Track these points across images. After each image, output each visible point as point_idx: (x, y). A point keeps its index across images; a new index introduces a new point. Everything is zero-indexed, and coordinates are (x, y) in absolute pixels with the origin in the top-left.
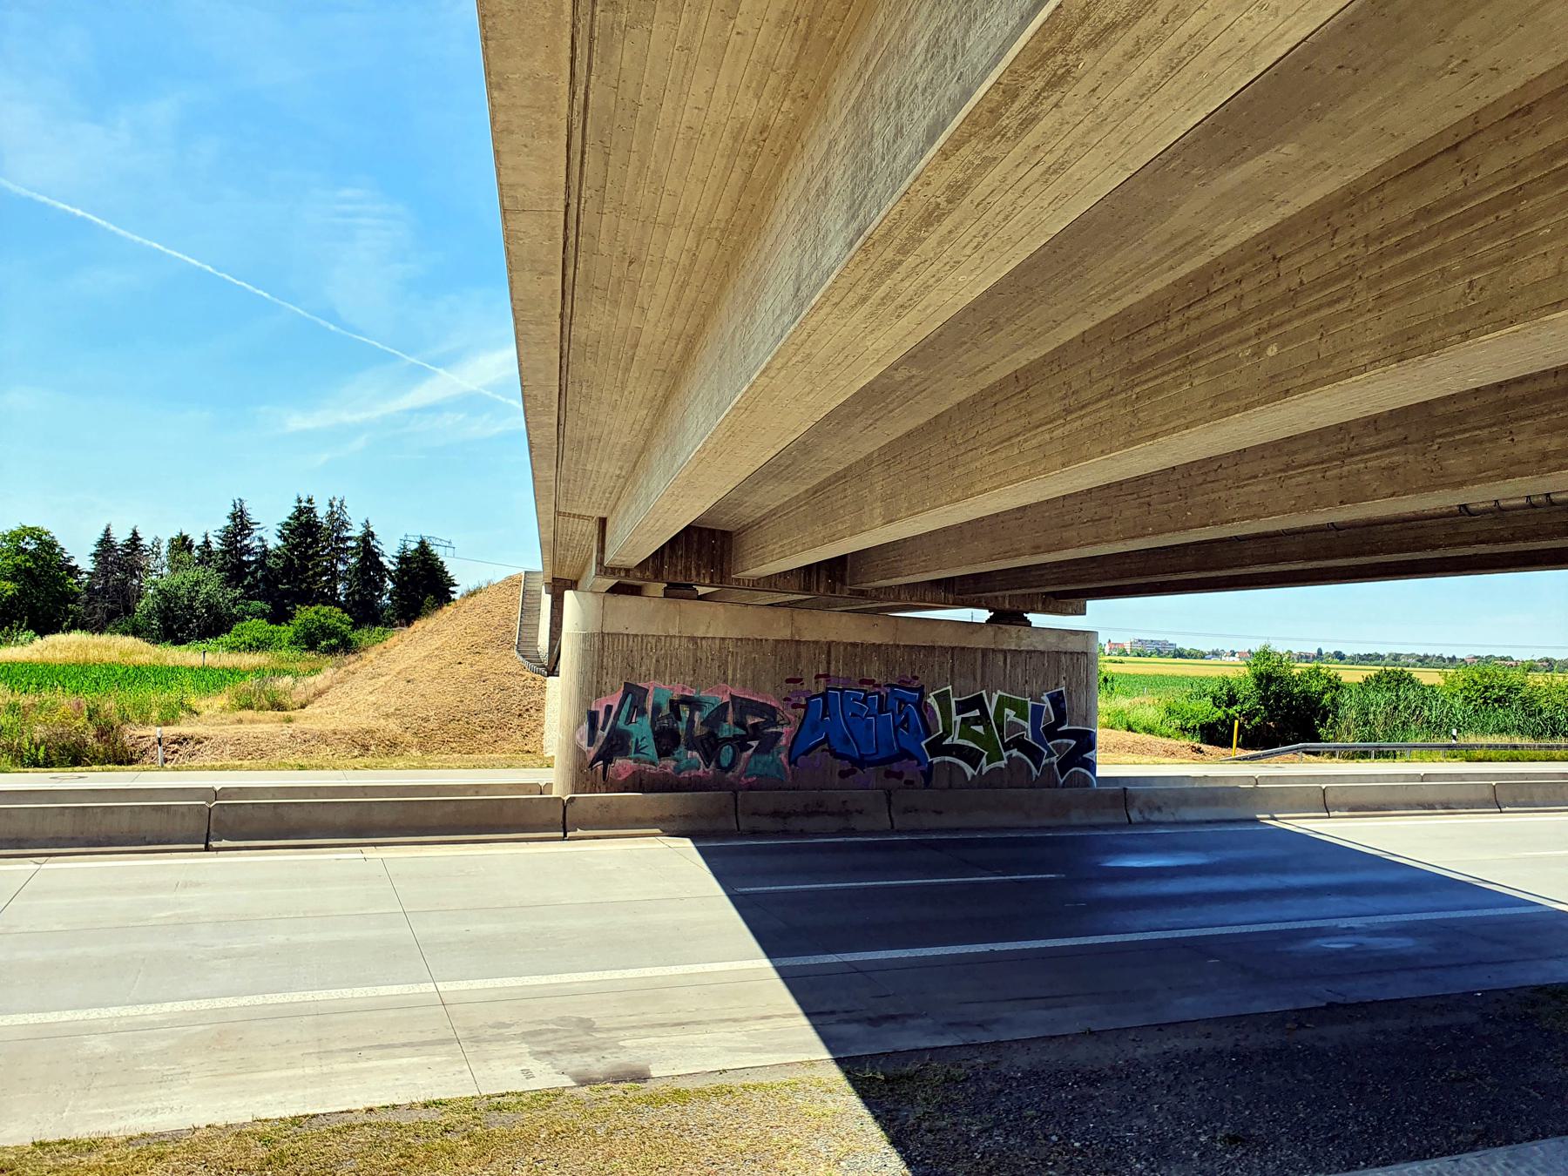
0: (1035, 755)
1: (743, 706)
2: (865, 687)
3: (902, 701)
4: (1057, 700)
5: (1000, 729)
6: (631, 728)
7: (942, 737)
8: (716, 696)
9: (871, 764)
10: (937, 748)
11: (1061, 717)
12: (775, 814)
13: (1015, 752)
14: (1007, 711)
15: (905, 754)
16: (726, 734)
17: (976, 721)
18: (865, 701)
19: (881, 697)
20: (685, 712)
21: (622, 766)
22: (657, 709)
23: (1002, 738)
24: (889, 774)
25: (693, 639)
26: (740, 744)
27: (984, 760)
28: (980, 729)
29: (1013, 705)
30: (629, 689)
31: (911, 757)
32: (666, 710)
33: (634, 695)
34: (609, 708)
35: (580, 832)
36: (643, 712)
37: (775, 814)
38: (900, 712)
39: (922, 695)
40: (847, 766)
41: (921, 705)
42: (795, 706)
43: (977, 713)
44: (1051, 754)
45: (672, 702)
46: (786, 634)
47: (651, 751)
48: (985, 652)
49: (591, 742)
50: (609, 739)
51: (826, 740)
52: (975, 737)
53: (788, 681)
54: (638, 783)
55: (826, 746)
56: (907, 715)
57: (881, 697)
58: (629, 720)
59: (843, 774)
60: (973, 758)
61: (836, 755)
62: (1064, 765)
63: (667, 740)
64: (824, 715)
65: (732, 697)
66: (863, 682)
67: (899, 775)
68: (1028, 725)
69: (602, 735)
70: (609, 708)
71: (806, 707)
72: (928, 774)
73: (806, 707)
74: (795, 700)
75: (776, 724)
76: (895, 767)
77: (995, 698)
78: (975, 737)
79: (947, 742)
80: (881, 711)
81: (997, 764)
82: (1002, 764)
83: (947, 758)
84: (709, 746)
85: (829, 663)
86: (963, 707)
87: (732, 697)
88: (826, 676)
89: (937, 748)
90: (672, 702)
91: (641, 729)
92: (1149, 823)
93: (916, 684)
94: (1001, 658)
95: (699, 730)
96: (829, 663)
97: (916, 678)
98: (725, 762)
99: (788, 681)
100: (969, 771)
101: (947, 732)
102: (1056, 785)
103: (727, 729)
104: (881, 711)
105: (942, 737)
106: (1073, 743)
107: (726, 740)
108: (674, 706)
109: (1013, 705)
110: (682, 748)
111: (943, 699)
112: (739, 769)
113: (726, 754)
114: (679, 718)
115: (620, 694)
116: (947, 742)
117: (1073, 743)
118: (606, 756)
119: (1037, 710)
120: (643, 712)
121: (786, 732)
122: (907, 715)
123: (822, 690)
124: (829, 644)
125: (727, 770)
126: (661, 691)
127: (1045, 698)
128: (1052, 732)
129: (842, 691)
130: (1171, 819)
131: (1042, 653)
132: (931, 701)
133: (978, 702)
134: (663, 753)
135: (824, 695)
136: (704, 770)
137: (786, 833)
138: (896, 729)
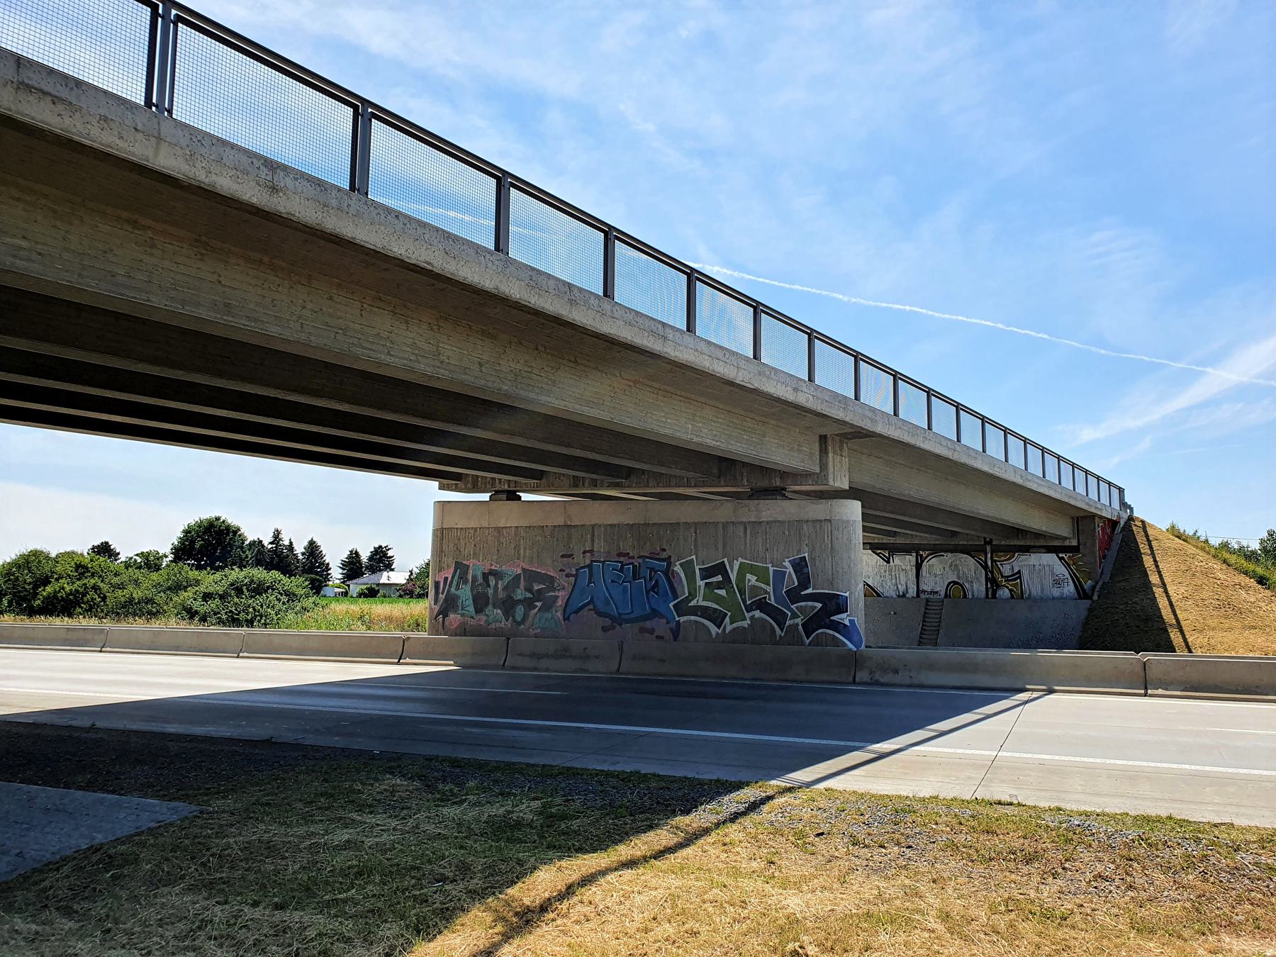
0: (779, 617)
1: (531, 576)
2: (622, 559)
3: (652, 569)
4: (799, 566)
5: (742, 592)
6: (458, 593)
7: (688, 600)
8: (513, 570)
9: (627, 621)
10: (682, 609)
11: (805, 581)
12: (534, 655)
13: (757, 614)
14: (748, 576)
15: (655, 614)
16: (519, 597)
17: (719, 586)
18: (621, 570)
19: (634, 567)
20: (492, 581)
21: (454, 618)
22: (475, 579)
23: (744, 602)
24: (642, 630)
25: (498, 529)
26: (529, 603)
27: (727, 619)
28: (723, 592)
29: (752, 569)
30: (458, 565)
31: (662, 616)
32: (480, 580)
33: (461, 568)
34: (446, 579)
35: (408, 660)
36: (466, 582)
37: (534, 655)
38: (651, 579)
39: (669, 565)
40: (608, 622)
41: (668, 573)
42: (567, 576)
43: (720, 578)
44: (794, 616)
45: (484, 574)
46: (561, 521)
47: (472, 609)
48: (725, 525)
49: (436, 603)
50: (446, 600)
51: (591, 601)
52: (718, 600)
53: (562, 556)
54: (463, 631)
55: (591, 607)
56: (657, 581)
57: (634, 567)
58: (457, 588)
59: (605, 629)
60: (717, 619)
61: (600, 614)
62: (809, 627)
63: (480, 603)
64: (590, 582)
65: (523, 569)
66: (620, 555)
67: (652, 631)
68: (770, 589)
69: (442, 597)
70: (446, 579)
71: (576, 576)
72: (676, 631)
73: (576, 576)
74: (568, 571)
75: (554, 590)
76: (648, 624)
77: (736, 567)
78: (718, 600)
79: (692, 604)
80: (635, 578)
81: (740, 624)
82: (745, 624)
83: (693, 618)
84: (508, 606)
85: (593, 541)
86: (707, 573)
87: (523, 569)
88: (591, 551)
89: (682, 609)
90: (484, 574)
91: (465, 593)
92: (877, 683)
93: (664, 555)
94: (742, 529)
95: (501, 595)
96: (593, 541)
97: (664, 550)
98: (519, 619)
99: (562, 556)
100: (714, 629)
101: (692, 595)
102: (803, 644)
103: (520, 594)
104: (635, 578)
105: (688, 600)
106: (819, 605)
107: (520, 601)
108: (485, 576)
109: (752, 569)
110: (490, 607)
111: (688, 567)
112: (528, 623)
113: (520, 611)
114: (489, 586)
115: (452, 570)
116: (692, 604)
117: (819, 605)
118: (444, 612)
119: (780, 575)
120: (466, 582)
121: (562, 595)
122: (657, 581)
123: (588, 562)
124: (593, 526)
125: (519, 624)
126: (477, 567)
127: (787, 564)
128: (794, 595)
129: (603, 562)
130: (908, 682)
131: (782, 522)
132: (678, 568)
133: (721, 569)
134: (479, 610)
135: (589, 566)
136: (505, 624)
137: (536, 669)
138: (648, 592)
